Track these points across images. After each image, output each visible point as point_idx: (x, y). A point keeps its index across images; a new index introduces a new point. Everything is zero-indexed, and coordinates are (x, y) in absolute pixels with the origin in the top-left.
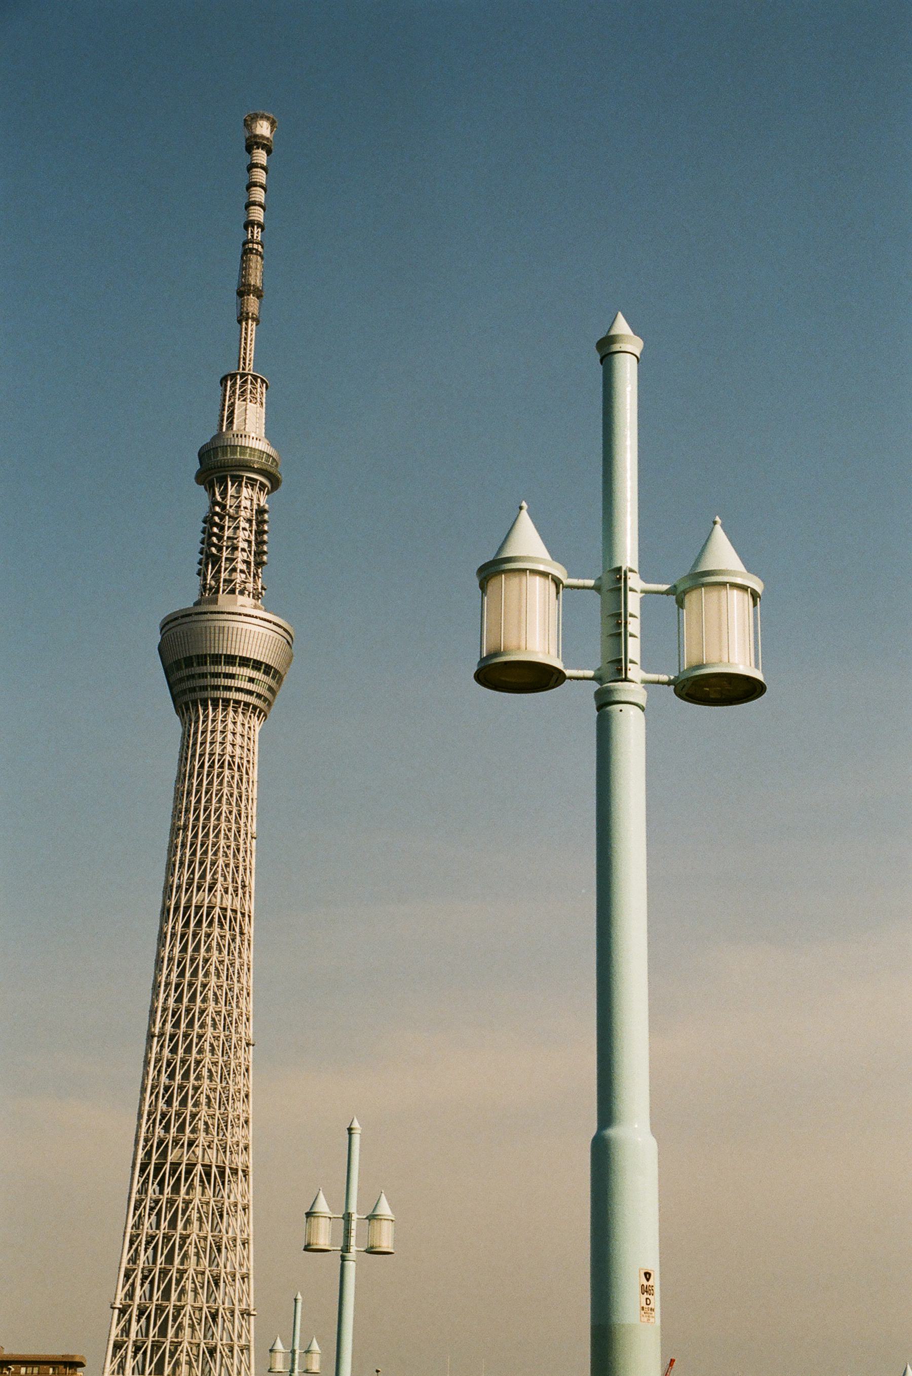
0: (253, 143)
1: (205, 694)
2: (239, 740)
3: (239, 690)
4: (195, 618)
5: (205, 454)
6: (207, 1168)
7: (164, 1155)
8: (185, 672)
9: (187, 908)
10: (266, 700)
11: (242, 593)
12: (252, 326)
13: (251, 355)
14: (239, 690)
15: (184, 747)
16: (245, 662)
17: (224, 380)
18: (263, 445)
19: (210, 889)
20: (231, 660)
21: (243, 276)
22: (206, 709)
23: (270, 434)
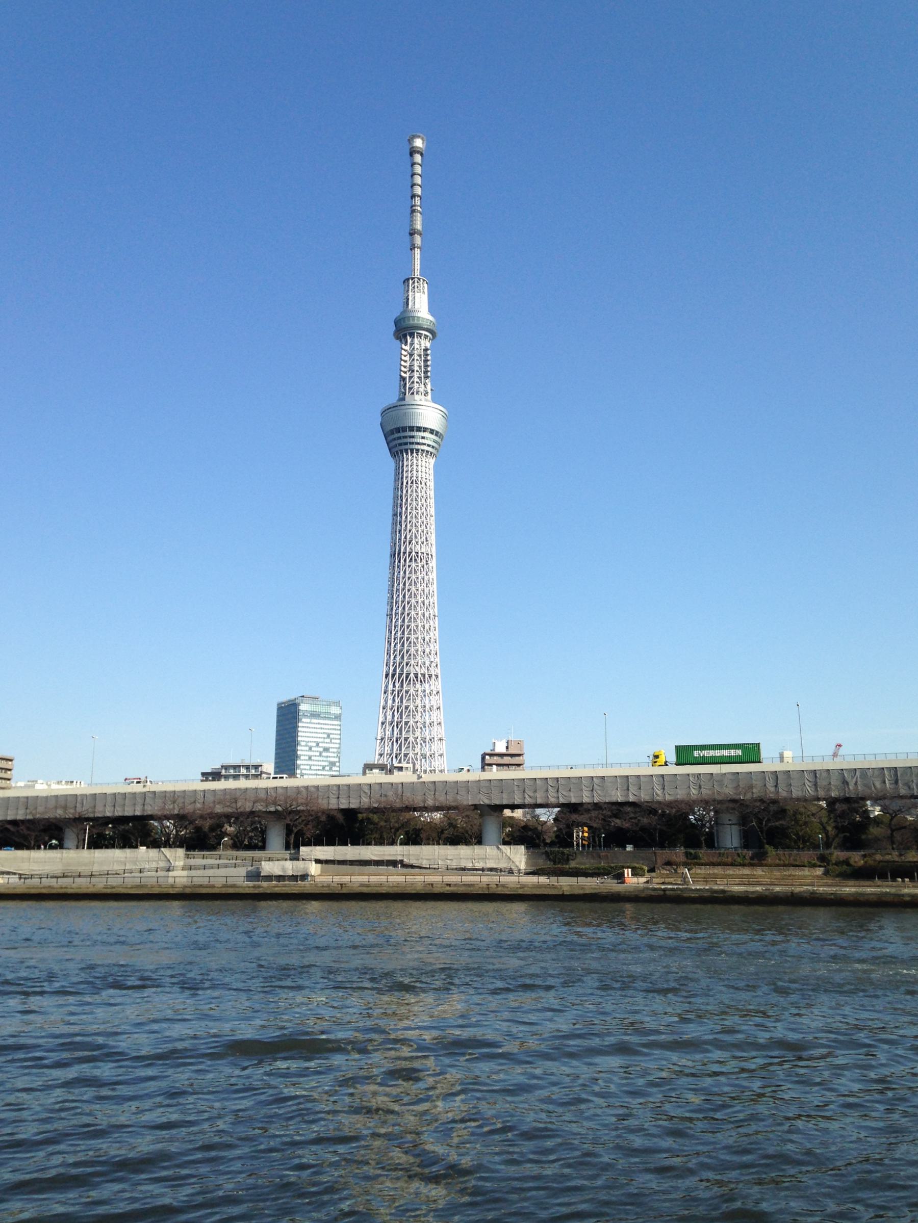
0: (412, 152)
1: (406, 447)
2: (424, 469)
3: (429, 446)
4: (408, 407)
5: (397, 322)
6: (416, 676)
7: (402, 670)
8: (397, 435)
9: (410, 553)
10: (436, 449)
11: (417, 393)
12: (417, 252)
13: (418, 266)
14: (429, 446)
15: (397, 474)
16: (432, 431)
17: (404, 282)
18: (431, 318)
19: (410, 543)
20: (425, 430)
21: (412, 225)
22: (407, 454)
23: (431, 311)
